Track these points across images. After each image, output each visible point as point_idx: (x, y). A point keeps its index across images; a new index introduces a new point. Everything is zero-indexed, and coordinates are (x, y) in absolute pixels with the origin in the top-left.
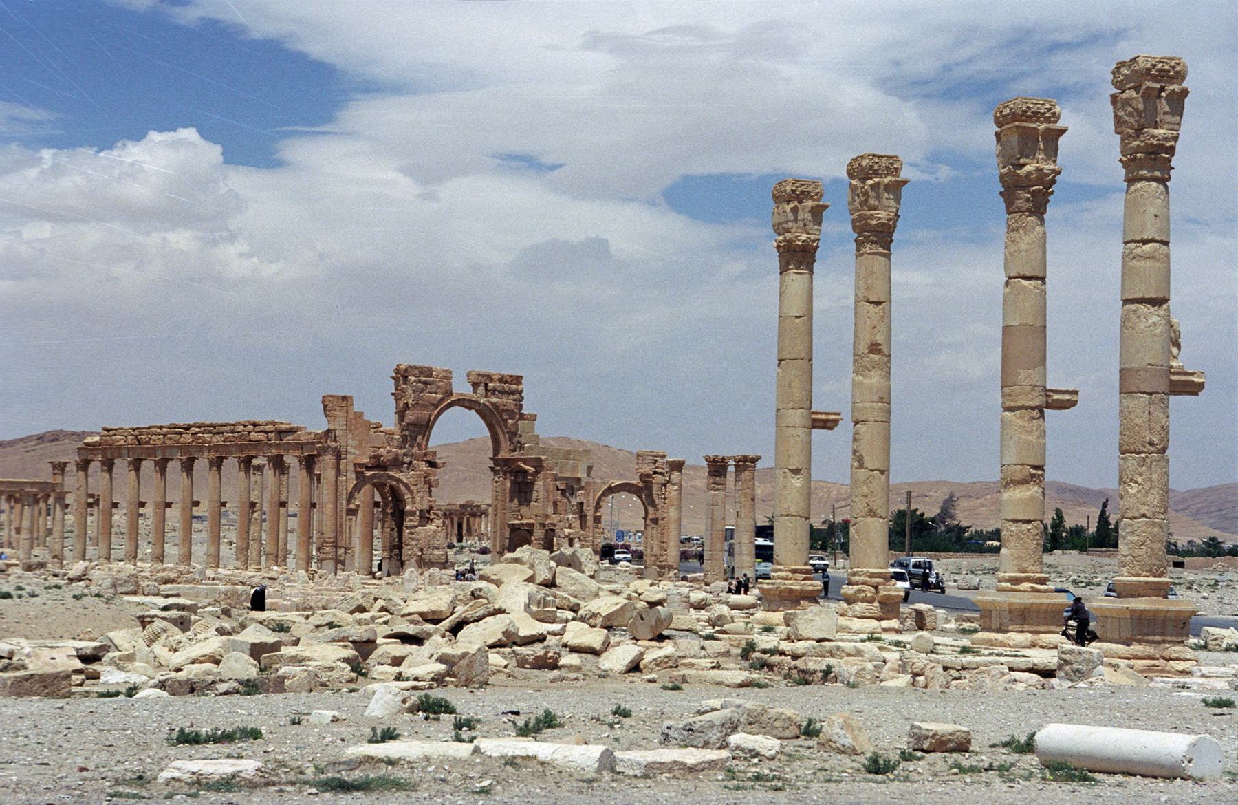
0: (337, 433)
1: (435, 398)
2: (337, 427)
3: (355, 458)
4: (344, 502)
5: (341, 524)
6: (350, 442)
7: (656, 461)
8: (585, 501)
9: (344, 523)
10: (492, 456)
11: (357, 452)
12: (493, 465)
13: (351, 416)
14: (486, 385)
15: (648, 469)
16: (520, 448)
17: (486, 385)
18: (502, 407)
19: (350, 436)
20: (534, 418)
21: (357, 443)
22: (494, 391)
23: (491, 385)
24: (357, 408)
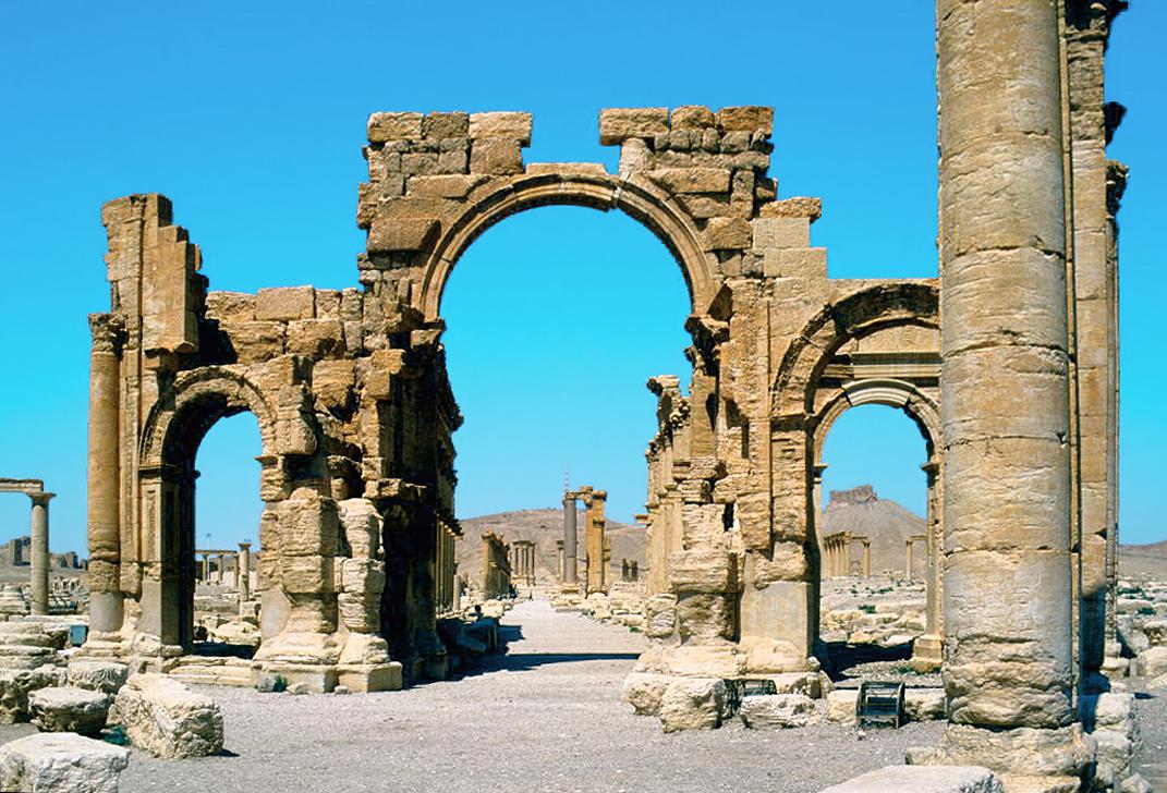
3: (158, 343)
4: (135, 452)
5: (129, 505)
6: (148, 304)
21: (163, 303)
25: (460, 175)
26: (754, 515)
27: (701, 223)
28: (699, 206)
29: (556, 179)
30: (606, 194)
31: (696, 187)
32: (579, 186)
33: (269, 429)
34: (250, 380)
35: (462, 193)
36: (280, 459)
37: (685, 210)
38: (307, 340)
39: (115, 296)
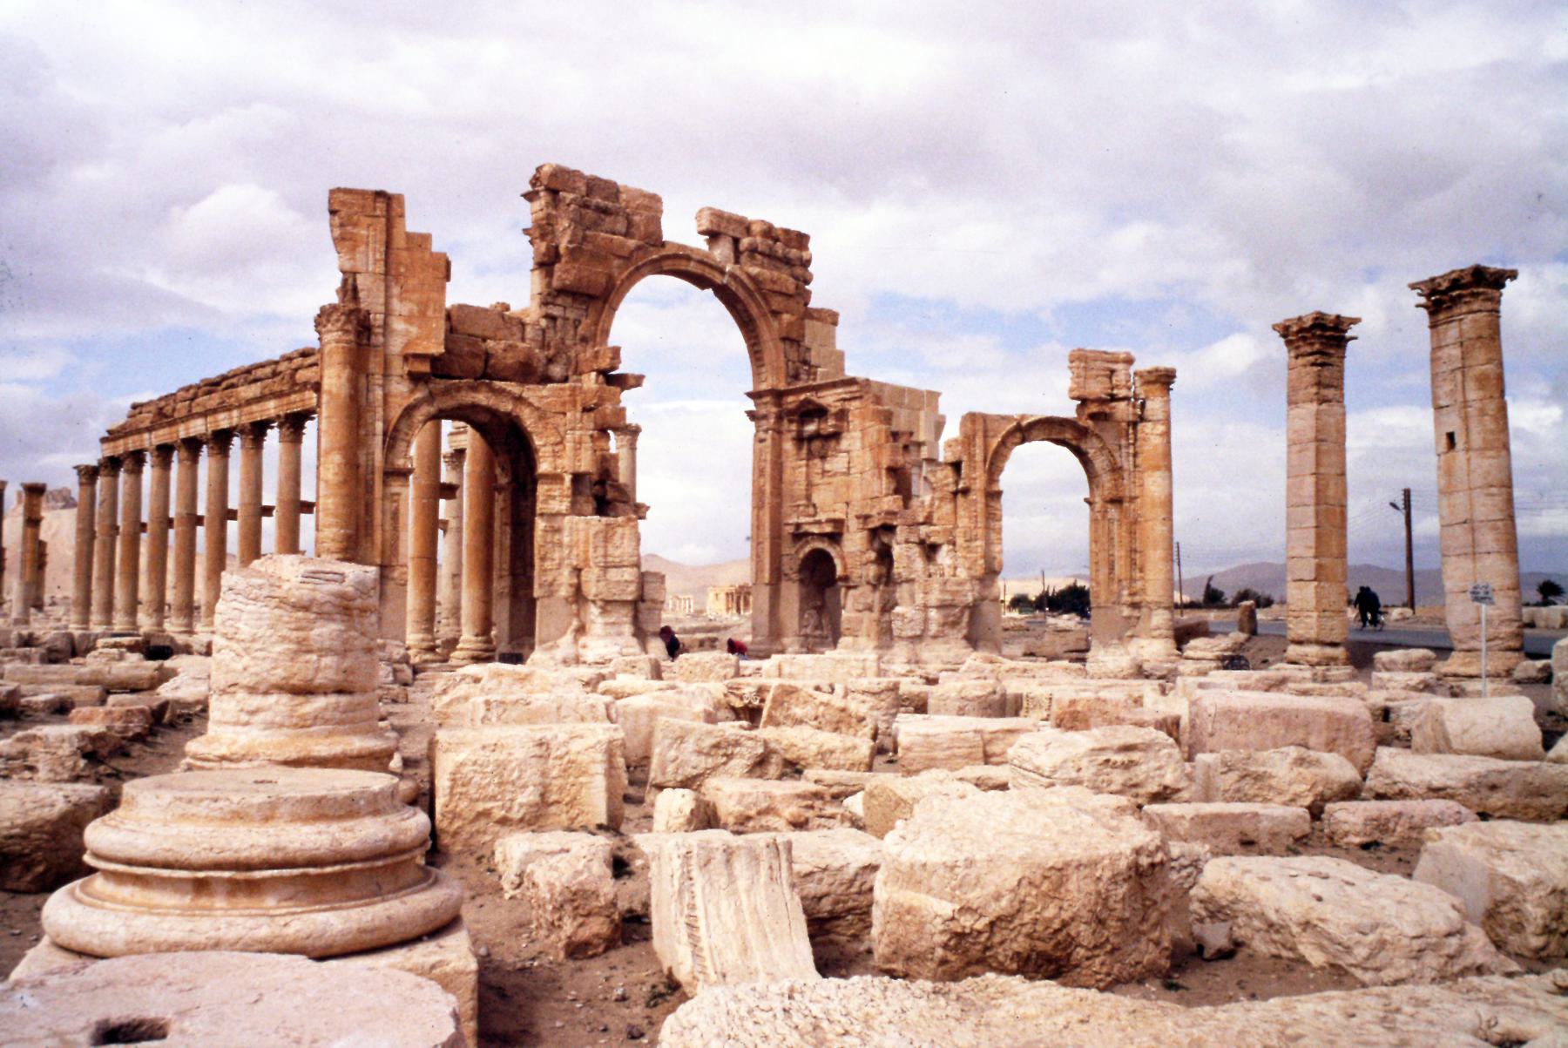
0: (360, 280)
1: (622, 246)
2: (360, 266)
3: (407, 345)
6: (396, 305)
7: (1112, 372)
8: (965, 458)
9: (378, 504)
10: (750, 388)
11: (414, 330)
12: (753, 408)
13: (399, 242)
14: (736, 241)
15: (1097, 388)
16: (809, 373)
17: (736, 241)
18: (769, 286)
19: (395, 290)
20: (831, 318)
21: (415, 308)
22: (753, 250)
23: (745, 242)
24: (413, 223)
25: (621, 238)
26: (974, 555)
27: (776, 314)
28: (777, 302)
29: (688, 258)
30: (718, 279)
31: (777, 288)
32: (702, 267)
33: (549, 448)
34: (531, 400)
35: (626, 254)
36: (568, 478)
37: (768, 303)
38: (510, 361)
39: (350, 287)
